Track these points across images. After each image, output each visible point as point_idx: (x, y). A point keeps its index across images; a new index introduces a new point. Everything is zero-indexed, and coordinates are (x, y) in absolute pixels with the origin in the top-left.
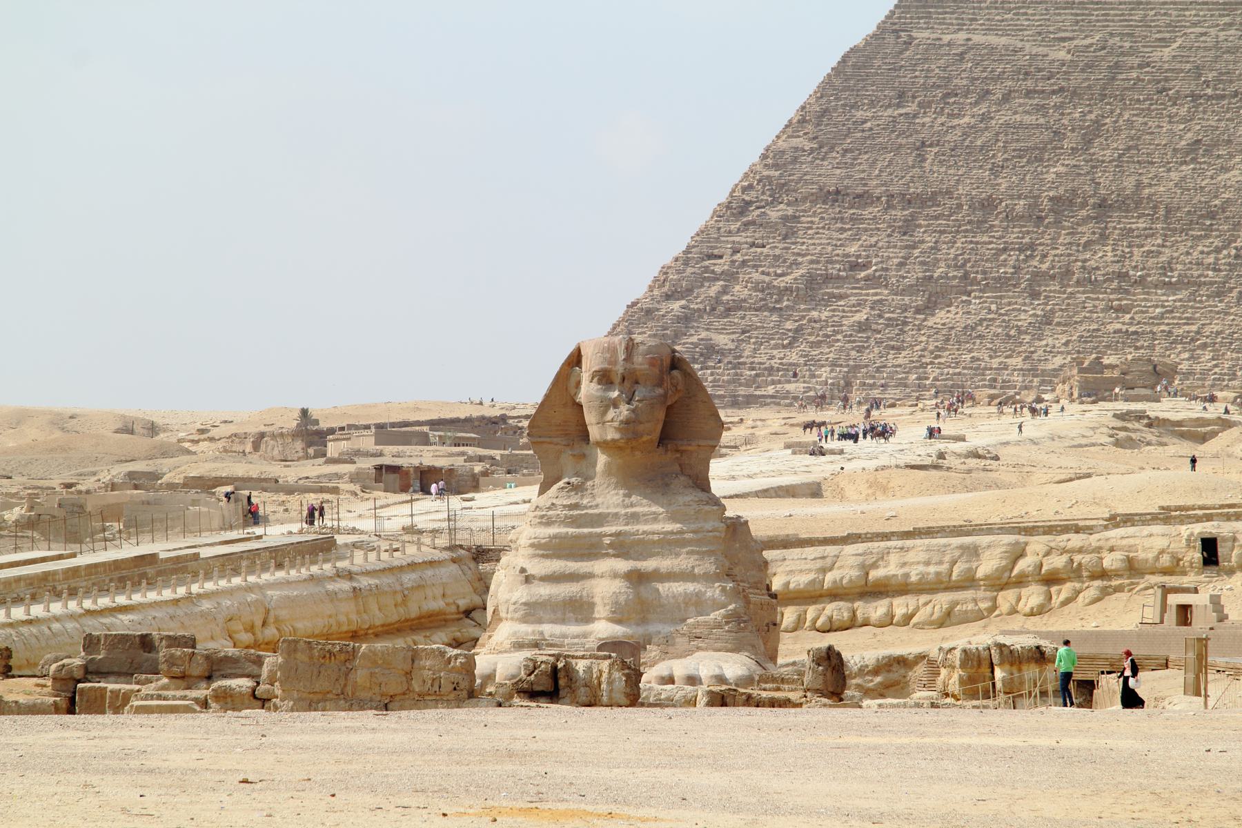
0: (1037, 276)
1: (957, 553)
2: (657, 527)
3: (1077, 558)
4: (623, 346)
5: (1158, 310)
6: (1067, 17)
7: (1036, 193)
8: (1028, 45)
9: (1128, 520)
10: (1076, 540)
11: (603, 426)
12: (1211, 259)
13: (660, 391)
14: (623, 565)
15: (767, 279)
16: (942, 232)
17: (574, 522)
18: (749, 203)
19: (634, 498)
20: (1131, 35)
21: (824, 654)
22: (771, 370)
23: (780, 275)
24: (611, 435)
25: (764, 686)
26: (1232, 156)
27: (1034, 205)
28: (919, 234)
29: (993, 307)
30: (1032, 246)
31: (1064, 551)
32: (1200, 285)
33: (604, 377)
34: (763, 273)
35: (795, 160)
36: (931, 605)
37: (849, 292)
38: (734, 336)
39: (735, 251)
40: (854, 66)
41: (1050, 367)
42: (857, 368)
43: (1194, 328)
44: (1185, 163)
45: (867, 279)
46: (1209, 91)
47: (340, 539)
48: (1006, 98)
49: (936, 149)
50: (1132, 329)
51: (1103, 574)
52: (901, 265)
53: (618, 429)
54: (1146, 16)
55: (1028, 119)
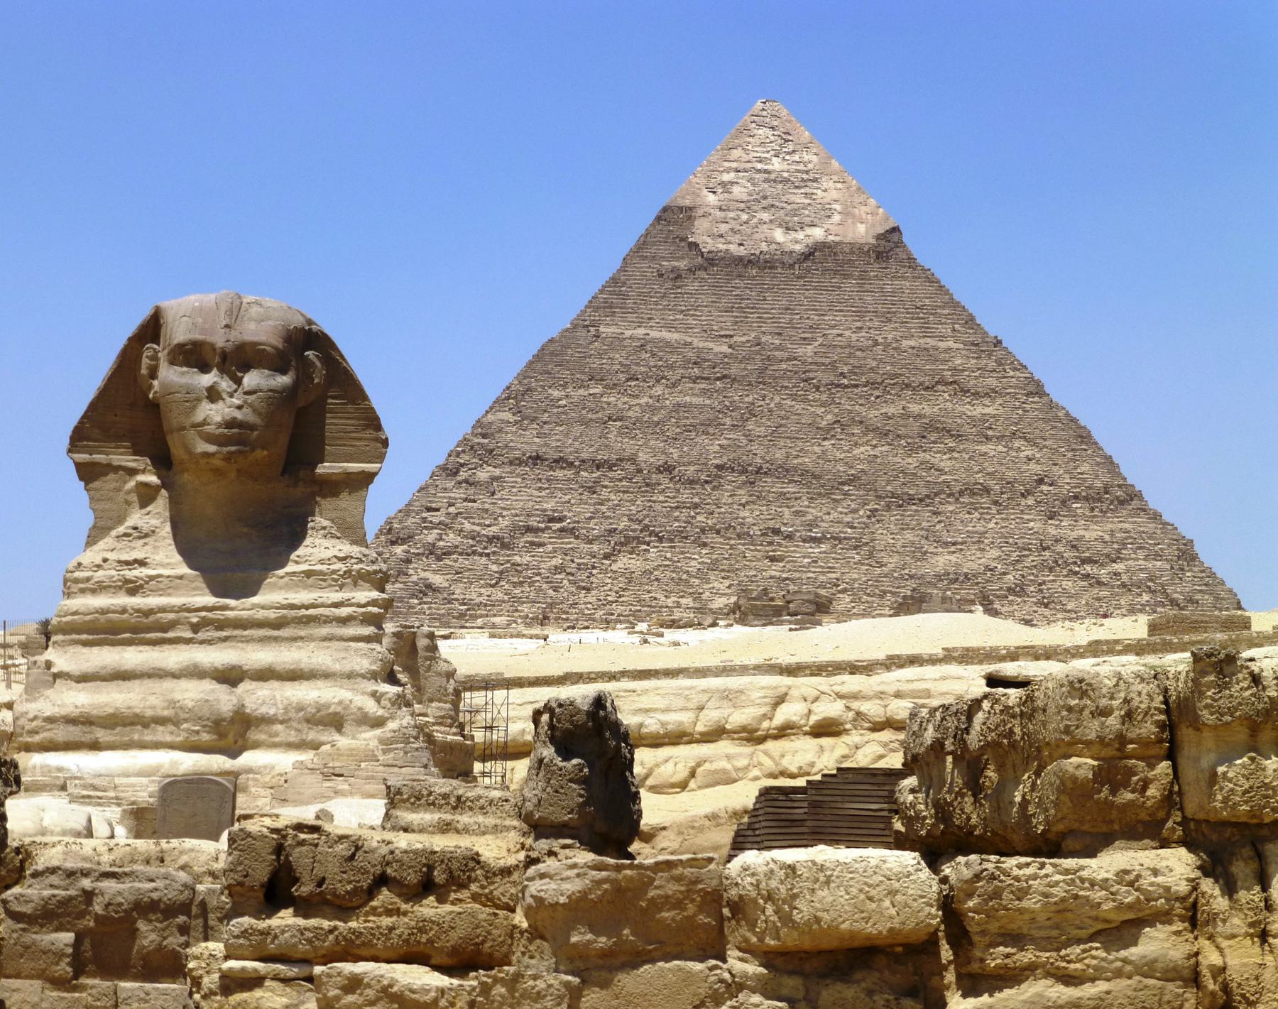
0: (703, 531)
1: (705, 697)
3: (855, 705)
5: (806, 560)
6: (728, 319)
7: (703, 461)
8: (695, 341)
9: (914, 660)
12: (848, 519)
13: (284, 380)
15: (477, 528)
16: (627, 492)
18: (462, 465)
20: (780, 334)
22: (479, 605)
23: (489, 526)
24: (203, 447)
25: (407, 816)
28: (604, 493)
29: (669, 555)
31: (840, 696)
32: (840, 540)
33: (194, 355)
34: (474, 524)
35: (500, 430)
36: (670, 766)
37: (546, 541)
38: (448, 577)
40: (552, 354)
41: (717, 606)
42: (551, 606)
43: (834, 576)
44: (825, 439)
45: (562, 530)
46: (845, 381)
49: (619, 423)
50: (785, 575)
52: (591, 518)
53: (210, 439)
54: (792, 320)
55: (696, 400)
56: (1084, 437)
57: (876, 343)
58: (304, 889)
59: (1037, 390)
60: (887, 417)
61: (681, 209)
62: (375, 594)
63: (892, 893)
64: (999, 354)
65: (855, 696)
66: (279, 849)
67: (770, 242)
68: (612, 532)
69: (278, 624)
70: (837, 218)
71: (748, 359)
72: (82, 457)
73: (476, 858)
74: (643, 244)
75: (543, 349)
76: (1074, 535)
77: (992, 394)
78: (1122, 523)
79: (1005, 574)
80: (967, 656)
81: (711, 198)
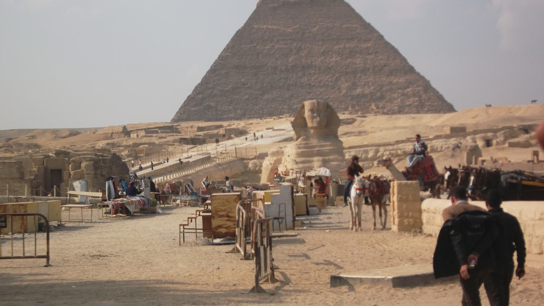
2: (327, 148)
3: (392, 152)
9: (403, 142)
10: (391, 148)
12: (330, 80)
14: (321, 158)
17: (306, 148)
22: (225, 111)
24: (315, 125)
26: (333, 54)
31: (388, 150)
39: (214, 82)
47: (212, 156)
48: (278, 41)
51: (398, 155)
52: (256, 83)
55: (284, 46)
57: (334, 26)
59: (381, 37)
60: (339, 49)
65: (393, 150)
75: (237, 32)
76: (395, 81)
77: (369, 40)
79: (376, 94)
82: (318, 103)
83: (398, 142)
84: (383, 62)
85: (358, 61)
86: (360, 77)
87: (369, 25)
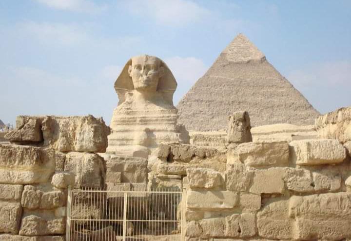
4: (145, 58)
9: (277, 132)
10: (265, 137)
11: (139, 82)
14: (144, 127)
17: (128, 114)
19: (148, 106)
21: (241, 117)
24: (141, 85)
27: (229, 103)
30: (229, 109)
33: (139, 67)
48: (224, 86)
55: (228, 89)
56: (301, 95)
58: (175, 158)
60: (264, 92)
61: (224, 54)
62: (175, 115)
63: (332, 150)
64: (285, 80)
65: (266, 139)
66: (170, 149)
67: (241, 59)
68: (212, 114)
69: (157, 120)
70: (253, 55)
71: (237, 81)
72: (117, 88)
73: (216, 150)
74: (217, 62)
75: (199, 80)
76: (300, 113)
77: (283, 87)
78: (309, 111)
80: (287, 131)
81: (230, 52)
82: (147, 57)
83: (273, 133)
84: (292, 101)
85: (276, 100)
86: (277, 110)
87: (284, 78)
